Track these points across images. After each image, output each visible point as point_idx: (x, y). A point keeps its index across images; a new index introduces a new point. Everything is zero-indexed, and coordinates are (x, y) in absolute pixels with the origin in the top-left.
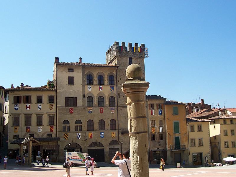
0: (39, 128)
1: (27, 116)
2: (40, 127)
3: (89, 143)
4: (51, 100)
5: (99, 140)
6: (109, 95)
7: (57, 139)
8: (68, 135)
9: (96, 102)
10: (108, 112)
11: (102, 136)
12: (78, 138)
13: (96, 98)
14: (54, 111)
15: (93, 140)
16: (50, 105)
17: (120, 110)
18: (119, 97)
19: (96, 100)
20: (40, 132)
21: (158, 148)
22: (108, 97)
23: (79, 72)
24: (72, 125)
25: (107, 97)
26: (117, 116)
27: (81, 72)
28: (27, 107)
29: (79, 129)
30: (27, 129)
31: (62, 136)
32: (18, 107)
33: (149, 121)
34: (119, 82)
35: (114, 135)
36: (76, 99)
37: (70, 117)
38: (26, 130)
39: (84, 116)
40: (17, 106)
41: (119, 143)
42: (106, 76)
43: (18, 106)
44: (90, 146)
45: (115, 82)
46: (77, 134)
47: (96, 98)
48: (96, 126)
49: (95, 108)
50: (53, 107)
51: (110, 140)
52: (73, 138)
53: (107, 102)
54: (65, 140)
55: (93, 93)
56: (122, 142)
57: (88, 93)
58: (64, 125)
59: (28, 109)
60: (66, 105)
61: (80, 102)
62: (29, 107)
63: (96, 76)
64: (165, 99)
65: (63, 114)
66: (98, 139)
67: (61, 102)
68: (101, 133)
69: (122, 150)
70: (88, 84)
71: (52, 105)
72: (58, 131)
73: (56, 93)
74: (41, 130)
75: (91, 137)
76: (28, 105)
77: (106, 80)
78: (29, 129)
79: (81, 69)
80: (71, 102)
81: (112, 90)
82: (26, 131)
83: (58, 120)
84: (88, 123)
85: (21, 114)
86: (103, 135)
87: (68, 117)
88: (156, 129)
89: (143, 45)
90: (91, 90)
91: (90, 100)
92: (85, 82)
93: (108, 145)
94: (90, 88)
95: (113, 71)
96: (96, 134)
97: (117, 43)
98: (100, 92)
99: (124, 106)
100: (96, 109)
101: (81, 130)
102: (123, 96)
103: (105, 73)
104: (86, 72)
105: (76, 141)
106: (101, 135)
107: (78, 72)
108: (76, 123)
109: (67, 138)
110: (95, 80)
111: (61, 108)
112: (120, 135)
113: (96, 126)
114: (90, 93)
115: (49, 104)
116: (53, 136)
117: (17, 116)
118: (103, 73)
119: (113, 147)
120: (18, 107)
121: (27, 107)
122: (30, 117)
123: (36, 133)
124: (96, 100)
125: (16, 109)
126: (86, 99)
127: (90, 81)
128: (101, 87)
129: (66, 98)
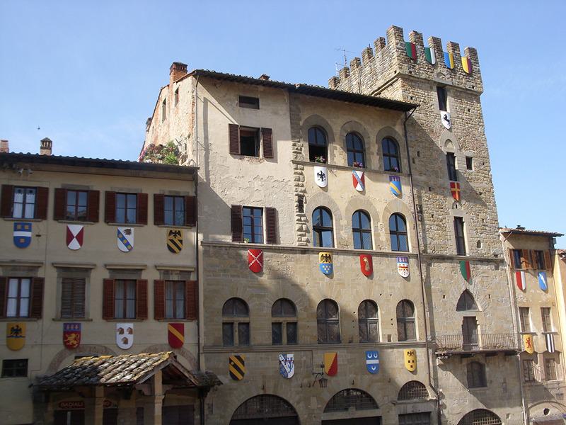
0: (122, 331)
1: (68, 275)
2: (126, 326)
3: (327, 397)
8: (243, 362)
11: (373, 365)
12: (283, 373)
14: (183, 260)
15: (340, 383)
16: (171, 233)
20: (131, 342)
21: (546, 411)
23: (281, 112)
25: (381, 218)
27: (285, 114)
28: (70, 237)
29: (284, 334)
30: (66, 333)
31: (221, 366)
32: (28, 234)
34: (414, 162)
37: (249, 287)
38: (65, 338)
40: (27, 227)
42: (373, 138)
43: (29, 230)
44: (332, 405)
45: (404, 162)
46: (282, 358)
50: (181, 241)
52: (264, 377)
53: (380, 236)
54: (235, 384)
58: (226, 319)
59: (75, 244)
61: (290, 233)
62: (80, 237)
63: (341, 135)
64: (549, 238)
65: (225, 271)
66: (359, 377)
68: (369, 353)
71: (179, 233)
72: (202, 342)
73: (196, 184)
74: (131, 338)
75: (333, 371)
76: (75, 229)
77: (375, 154)
78: (78, 332)
82: (61, 341)
83: (206, 298)
85: (42, 263)
86: (376, 362)
89: (473, 52)
91: (322, 221)
95: (395, 125)
97: (399, 32)
101: (293, 338)
103: (367, 127)
105: (276, 386)
106: (368, 362)
107: (276, 113)
108: (274, 313)
109: (242, 374)
118: (361, 125)
120: (28, 234)
121: (70, 237)
122: (83, 282)
125: (22, 241)
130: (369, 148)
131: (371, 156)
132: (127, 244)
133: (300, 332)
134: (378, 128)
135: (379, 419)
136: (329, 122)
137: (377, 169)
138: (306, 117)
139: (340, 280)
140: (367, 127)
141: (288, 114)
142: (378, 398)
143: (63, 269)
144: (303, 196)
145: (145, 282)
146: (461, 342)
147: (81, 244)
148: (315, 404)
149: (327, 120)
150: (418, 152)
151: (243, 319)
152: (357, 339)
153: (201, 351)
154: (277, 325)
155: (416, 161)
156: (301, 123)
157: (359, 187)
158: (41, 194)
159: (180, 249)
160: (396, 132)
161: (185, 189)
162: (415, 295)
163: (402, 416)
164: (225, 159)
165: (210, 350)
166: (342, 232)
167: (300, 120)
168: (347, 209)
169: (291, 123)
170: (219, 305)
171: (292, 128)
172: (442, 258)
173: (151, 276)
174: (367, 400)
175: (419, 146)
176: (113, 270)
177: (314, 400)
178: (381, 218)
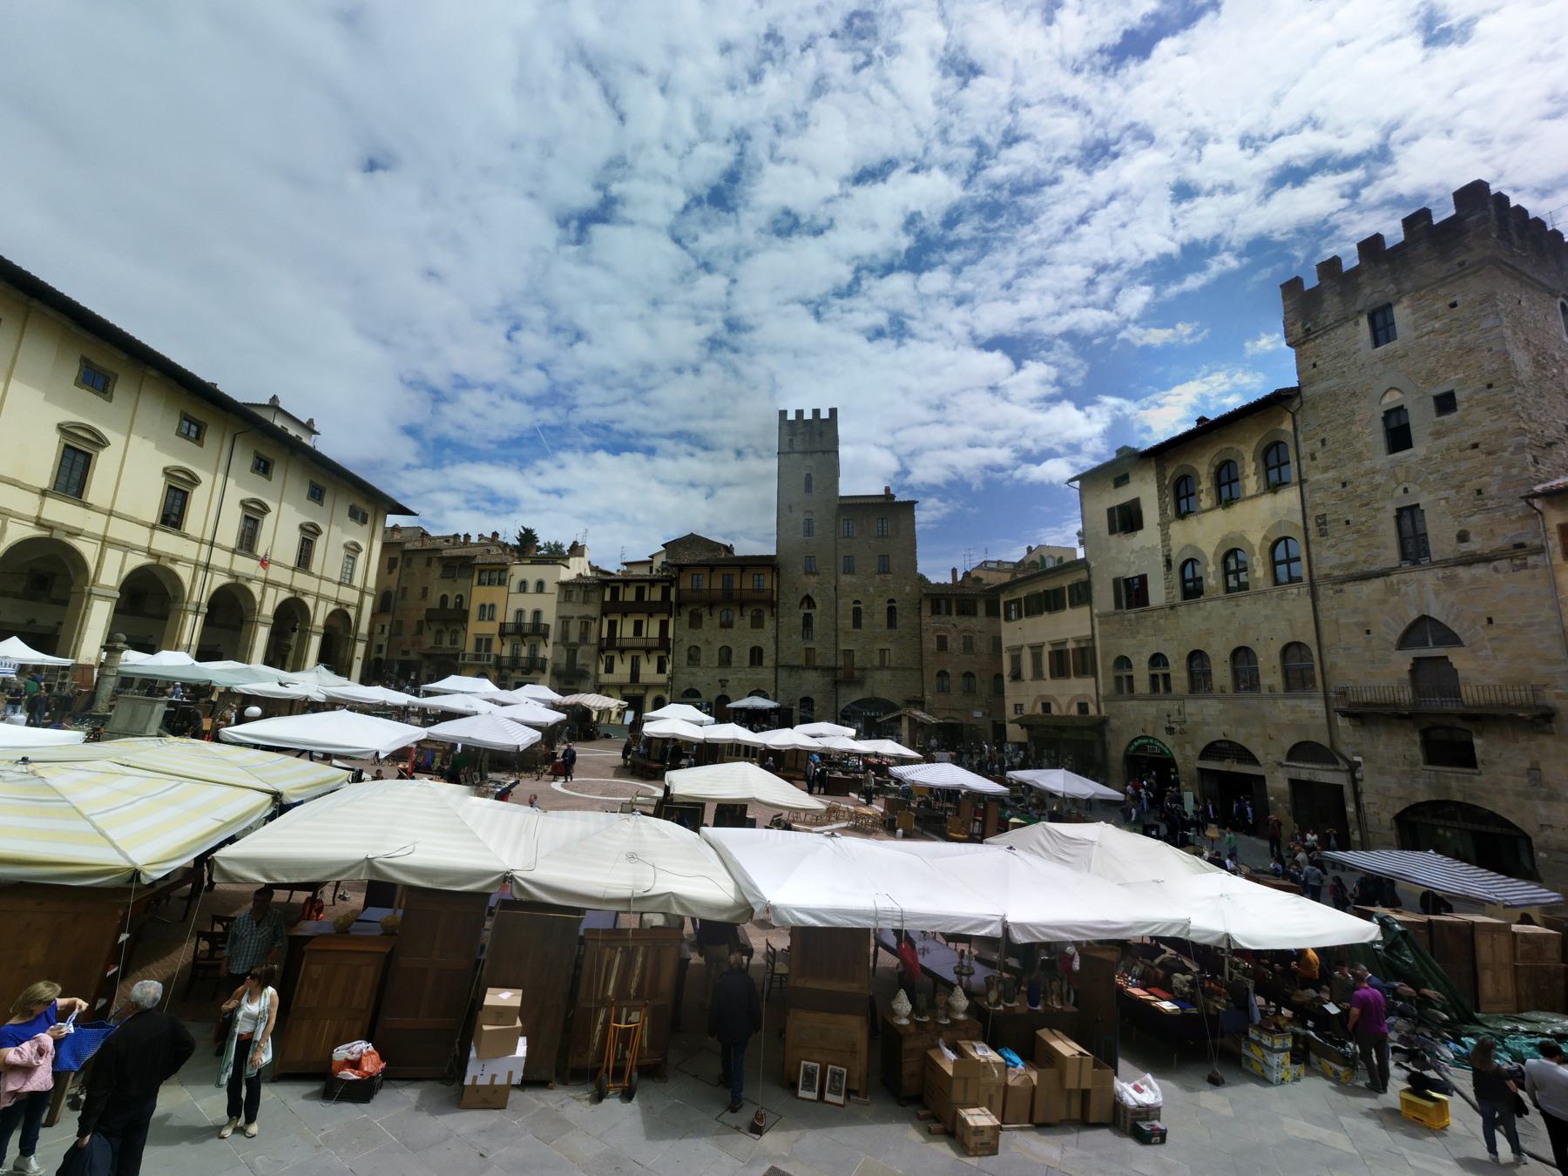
3: (1201, 746)
5: (1239, 736)
6: (1265, 538)
7: (1101, 724)
9: (1214, 578)
13: (1211, 562)
18: (1323, 533)
19: (1211, 569)
22: (1260, 549)
24: (1141, 674)
26: (1312, 626)
34: (1313, 457)
35: (1306, 715)
36: (1143, 579)
39: (1172, 639)
41: (1338, 757)
42: (1249, 457)
47: (1211, 562)
48: (1221, 673)
49: (1209, 604)
51: (1288, 745)
55: (1200, 545)
56: (1357, 759)
58: (1118, 674)
60: (1118, 604)
61: (1158, 593)
63: (1208, 473)
67: (1104, 596)
69: (1365, 800)
70: (1181, 515)
80: (1133, 592)
83: (1102, 658)
84: (1194, 664)
87: (1127, 647)
92: (1170, 512)
93: (1281, 765)
95: (1281, 423)
96: (1221, 707)
101: (1168, 688)
102: (1348, 522)
104: (1170, 473)
111: (1104, 617)
112: (1342, 722)
113: (1221, 673)
116: (1092, 710)
117: (1016, 653)
118: (1233, 448)
119: (1304, 776)
123: (1055, 700)
124: (1211, 569)
126: (1175, 575)
129: (1116, 582)
130: (1243, 473)
131: (1246, 481)
133: (1173, 683)
134: (1254, 445)
135: (1262, 778)
136: (1195, 466)
137: (1254, 493)
140: (1242, 447)
142: (1259, 754)
143: (1032, 647)
145: (1068, 650)
146: (1406, 695)
148: (1192, 751)
150: (1323, 442)
151: (1128, 673)
152: (1229, 690)
153: (1100, 699)
154: (1154, 678)
155: (1318, 455)
156: (1167, 482)
158: (1018, 601)
160: (1283, 431)
161: (1083, 575)
162: (1308, 638)
163: (1294, 783)
165: (1107, 699)
166: (1212, 576)
167: (1165, 479)
168: (1215, 554)
169: (1158, 487)
170: (1111, 662)
171: (1159, 491)
172: (1366, 577)
173: (1071, 646)
174: (1245, 756)
175: (1324, 431)
176: (1053, 644)
177: (1188, 746)
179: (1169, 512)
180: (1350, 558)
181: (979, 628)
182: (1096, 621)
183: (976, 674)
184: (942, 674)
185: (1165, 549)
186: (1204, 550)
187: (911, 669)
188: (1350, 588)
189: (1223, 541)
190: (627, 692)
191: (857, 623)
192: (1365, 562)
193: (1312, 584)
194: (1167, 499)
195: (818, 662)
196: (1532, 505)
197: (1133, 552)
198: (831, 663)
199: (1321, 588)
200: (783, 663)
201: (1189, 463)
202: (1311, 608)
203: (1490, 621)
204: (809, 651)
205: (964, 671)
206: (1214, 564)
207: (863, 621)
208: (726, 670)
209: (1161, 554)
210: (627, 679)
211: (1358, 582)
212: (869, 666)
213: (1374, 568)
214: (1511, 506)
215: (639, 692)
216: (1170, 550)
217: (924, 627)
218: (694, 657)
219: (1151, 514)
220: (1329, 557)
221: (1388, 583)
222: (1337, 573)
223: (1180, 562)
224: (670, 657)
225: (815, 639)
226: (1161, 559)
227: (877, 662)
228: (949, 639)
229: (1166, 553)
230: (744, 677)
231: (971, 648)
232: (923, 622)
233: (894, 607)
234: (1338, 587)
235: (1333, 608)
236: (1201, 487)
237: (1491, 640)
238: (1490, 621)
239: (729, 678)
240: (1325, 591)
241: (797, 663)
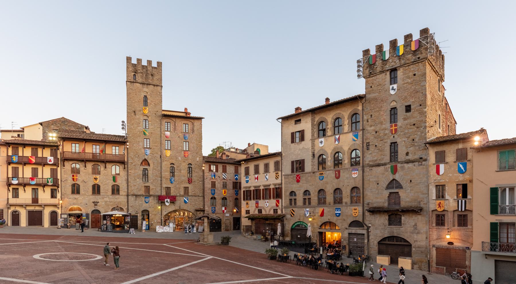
4: (278, 166)
6: (349, 149)
9: (330, 162)
10: (348, 176)
13: (329, 157)
17: (368, 170)
18: (368, 149)
22: (347, 153)
23: (308, 121)
25: (346, 153)
32: (248, 179)
33: (430, 187)
43: (248, 178)
47: (329, 157)
55: (326, 149)
57: (319, 151)
59: (256, 180)
76: (256, 176)
79: (311, 116)
81: (356, 139)
88: (449, 203)
90: (323, 145)
92: (316, 135)
94: (321, 142)
98: (336, 146)
99: (378, 162)
100: (329, 174)
107: (306, 122)
110: (328, 128)
114: (322, 149)
115: (275, 173)
120: (248, 179)
124: (329, 159)
127: (322, 132)
128: (337, 137)
132: (267, 179)
138: (317, 119)
139: (326, 182)
141: (311, 121)
144: (314, 152)
147: (257, 179)
149: (325, 117)
156: (315, 123)
157: (337, 143)
159: (278, 178)
164: (290, 145)
166: (330, 162)
168: (331, 153)
171: (312, 126)
172: (379, 165)
173: (272, 187)
178: (346, 153)
179: (315, 135)
180: (375, 158)
181: (229, 178)
182: (283, 177)
183: (228, 198)
184: (213, 198)
185: (313, 150)
186: (327, 151)
187: (199, 196)
188: (374, 169)
189: (334, 149)
190: (31, 208)
191: (173, 173)
192: (380, 160)
193: (363, 167)
194: (315, 130)
195: (151, 193)
196: (426, 145)
197: (300, 149)
198: (159, 194)
199: (366, 168)
200: (132, 193)
201: (324, 116)
202: (362, 175)
203: (411, 181)
204: (147, 188)
205: (222, 197)
206: (330, 157)
207: (175, 173)
208: (97, 196)
209: (311, 151)
210: (30, 202)
211: (377, 167)
212: (178, 195)
213: (382, 162)
214: (421, 145)
215: (37, 208)
216: (314, 150)
217: (205, 177)
218: (96, 189)
219: (308, 135)
220: (369, 158)
221: (386, 168)
222: (371, 163)
223: (318, 155)
224: (60, 189)
225: (149, 181)
226: (311, 154)
227: (182, 193)
228: (216, 182)
229: (313, 151)
230: (108, 200)
231: (226, 187)
232: (205, 175)
233: (191, 167)
234: (371, 168)
235: (368, 176)
236: (328, 127)
237: (411, 187)
238: (411, 181)
239: (99, 201)
240: (367, 169)
241: (139, 193)
